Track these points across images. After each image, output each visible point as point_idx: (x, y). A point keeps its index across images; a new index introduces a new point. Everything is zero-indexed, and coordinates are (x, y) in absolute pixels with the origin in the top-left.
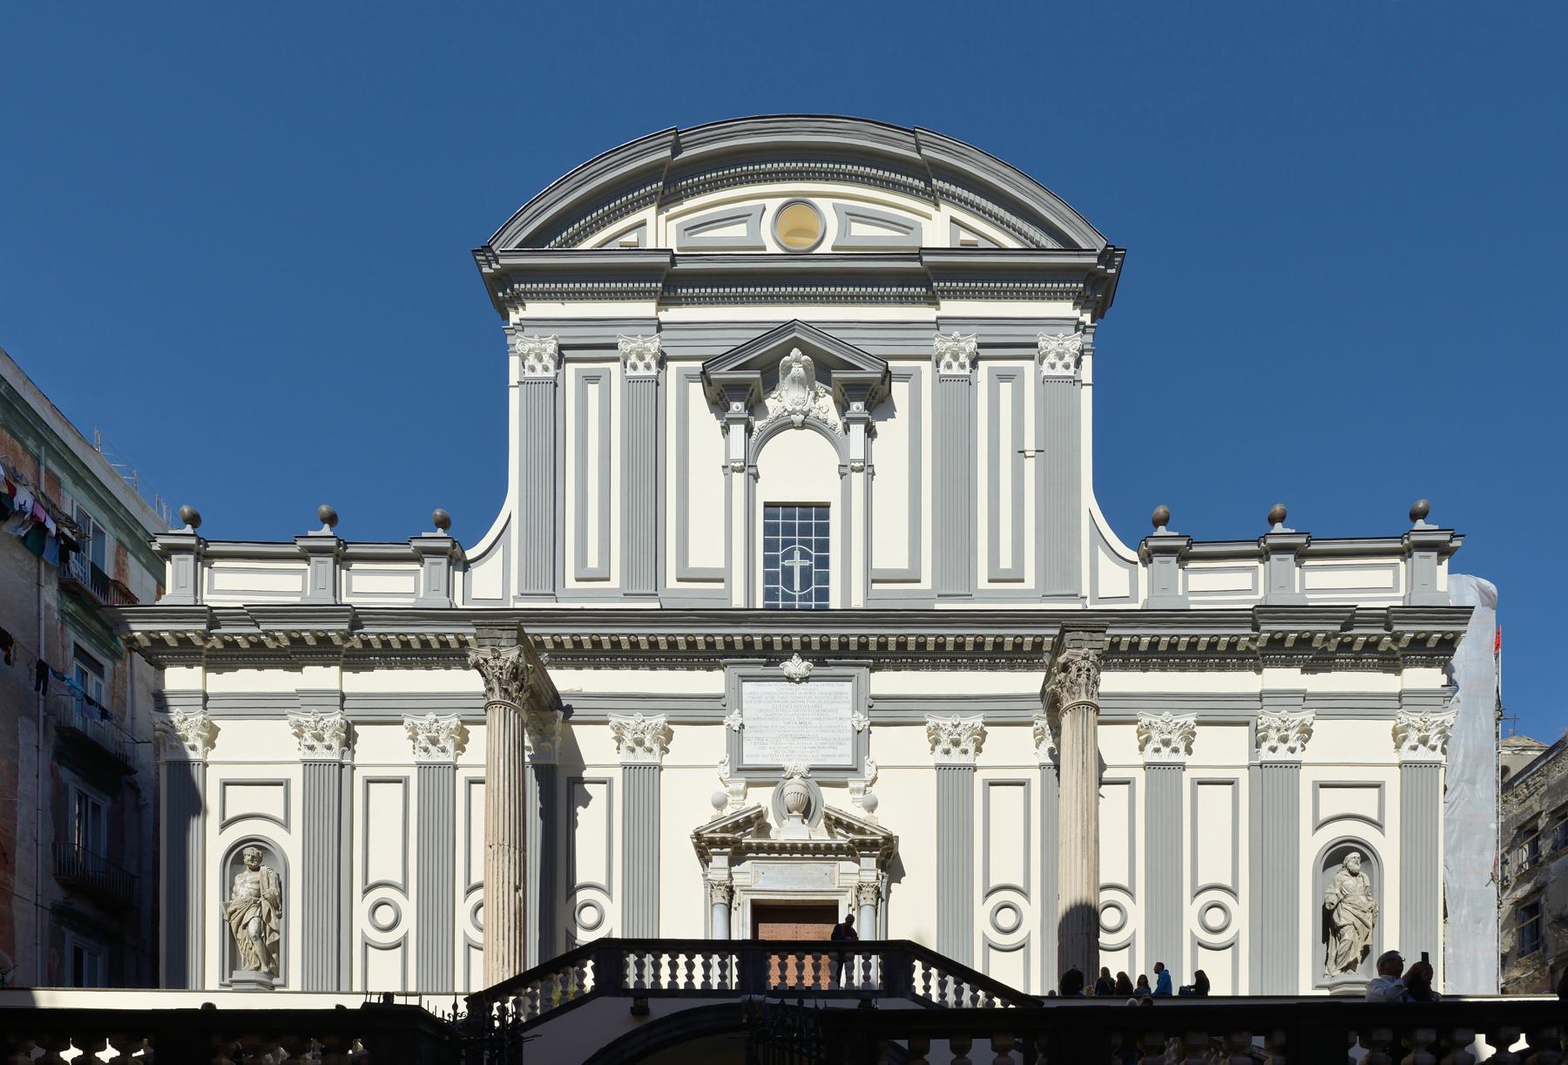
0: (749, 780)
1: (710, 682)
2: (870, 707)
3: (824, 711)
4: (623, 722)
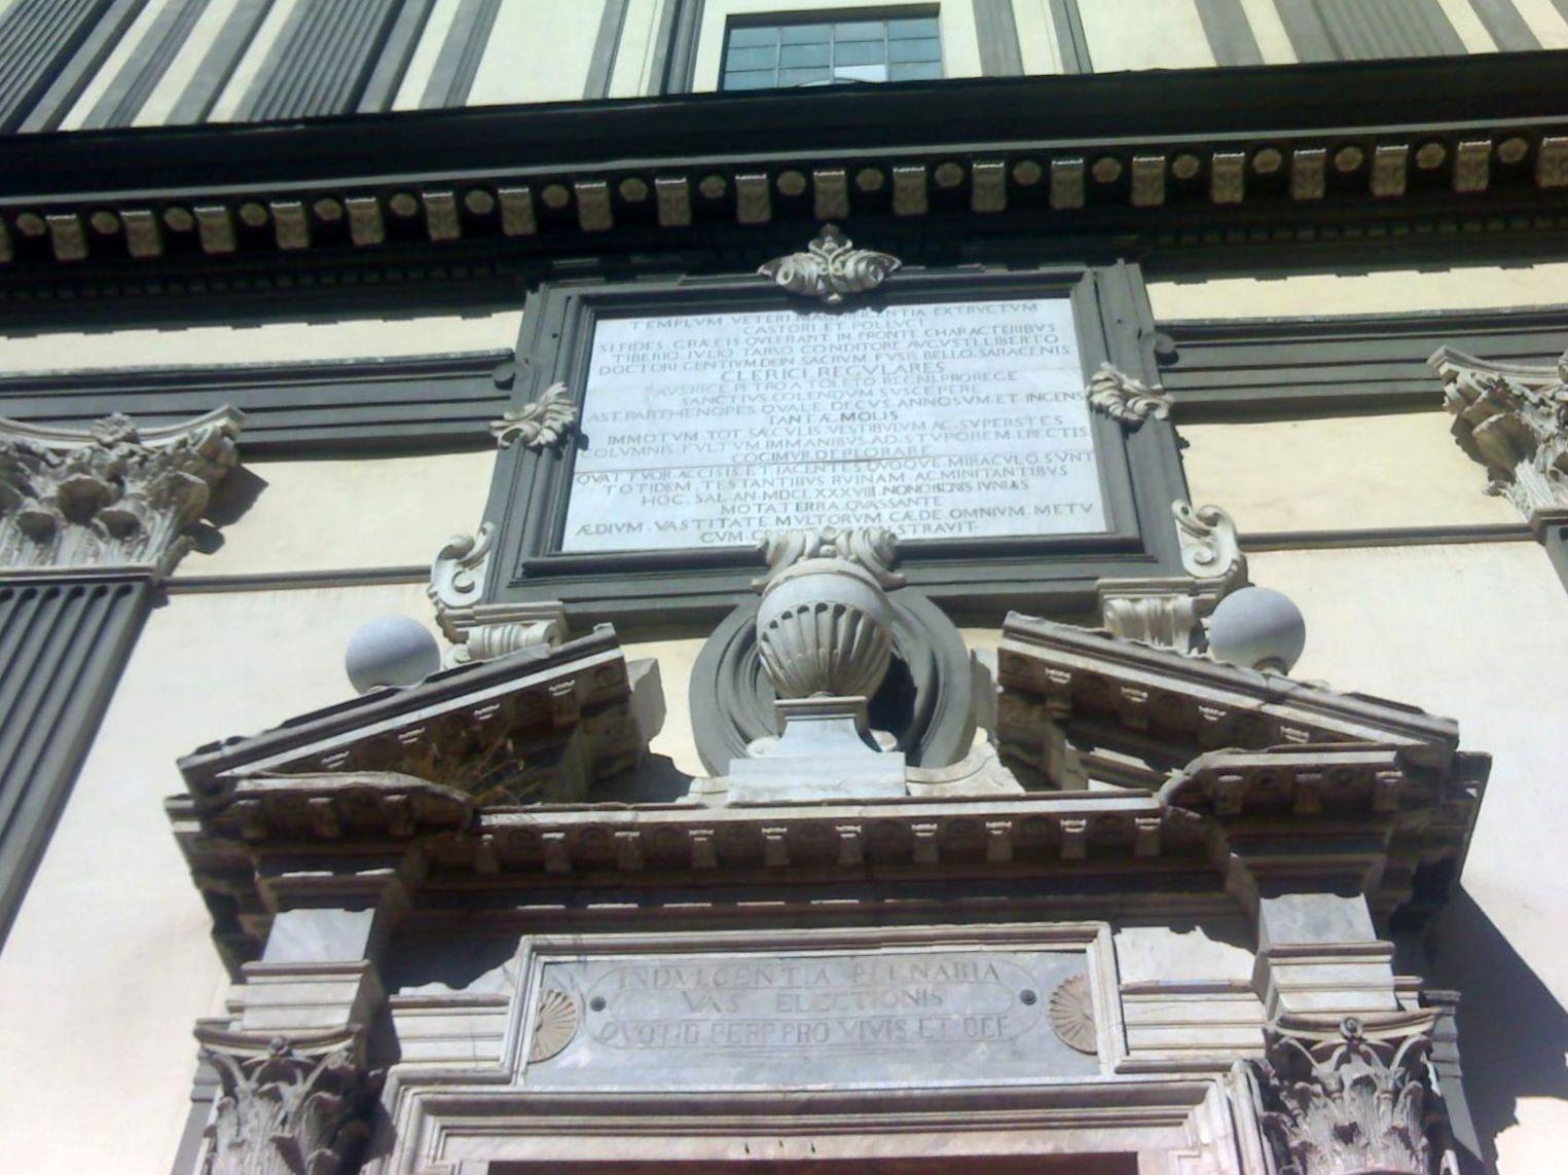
0: (573, 609)
3: (956, 377)
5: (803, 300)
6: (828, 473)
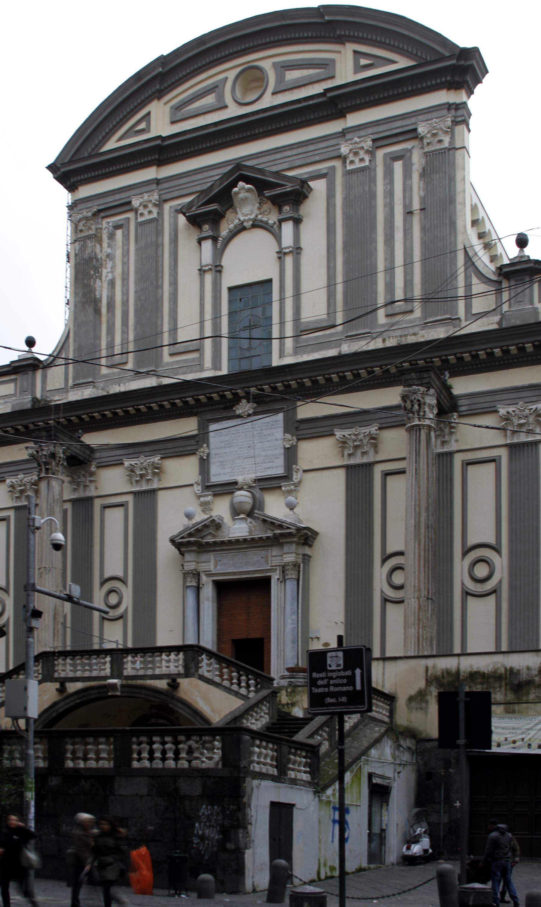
2: (296, 428)
3: (265, 436)
4: (133, 463)
5: (239, 416)
6: (246, 461)
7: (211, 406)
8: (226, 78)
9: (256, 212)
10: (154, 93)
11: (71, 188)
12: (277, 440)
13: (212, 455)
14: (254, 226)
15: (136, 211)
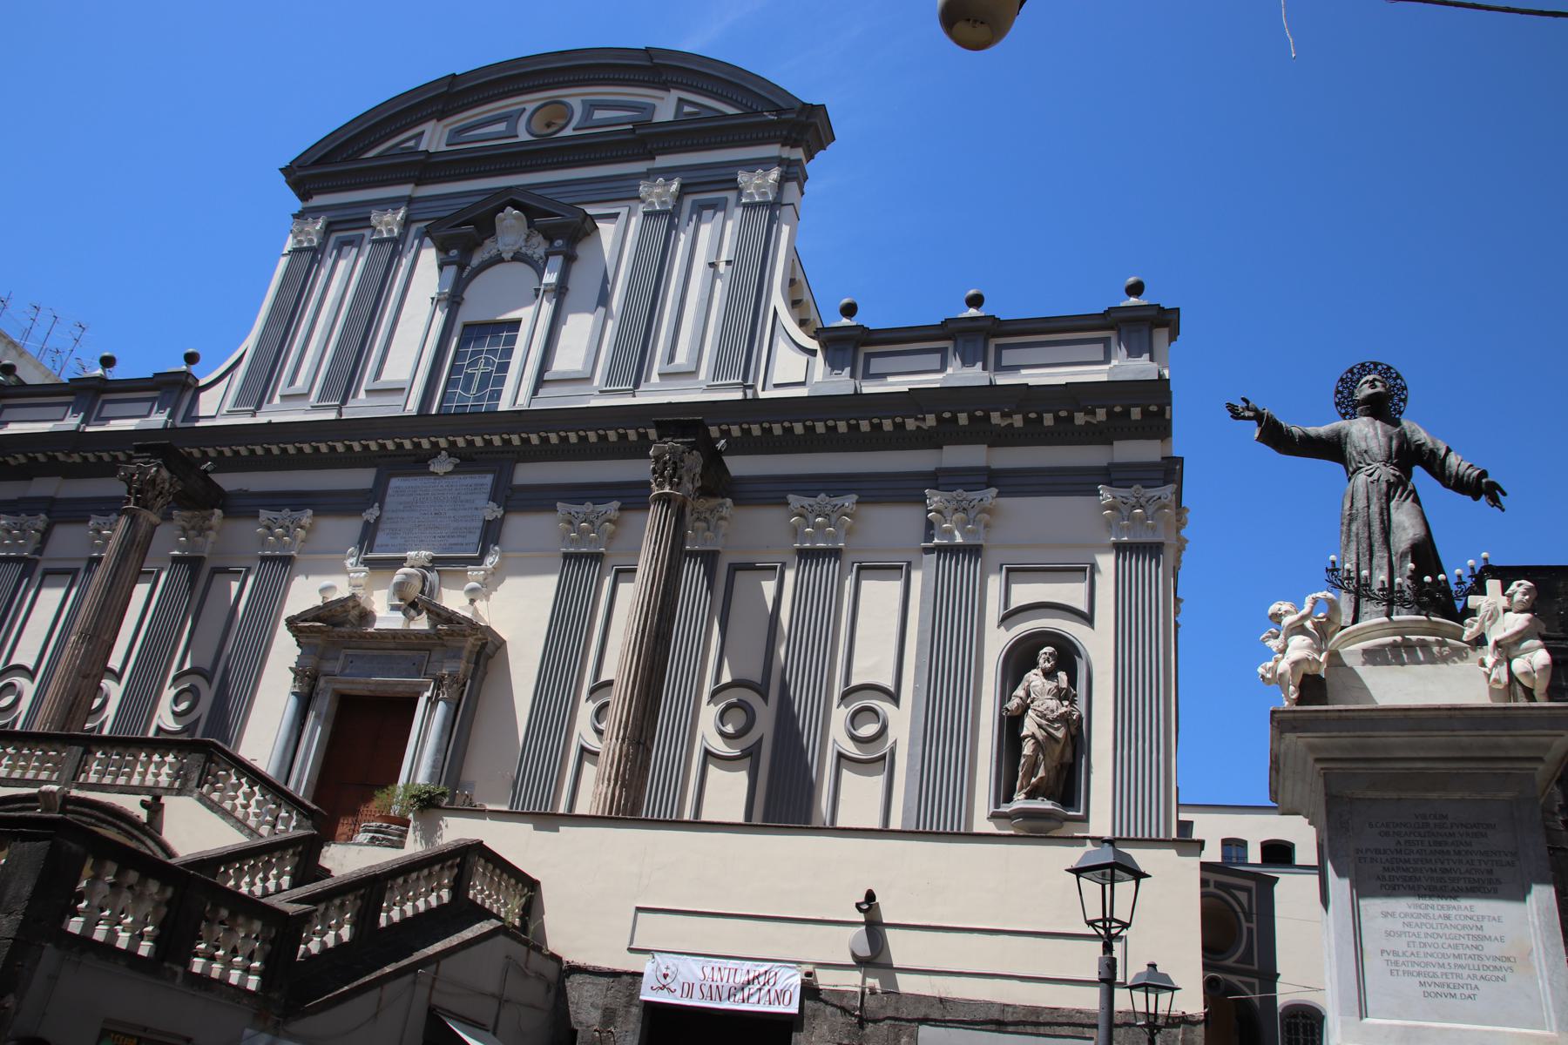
1: (362, 478)
3: (462, 502)
7: (399, 456)
8: (524, 109)
9: (521, 243)
10: (433, 113)
11: (304, 197)
12: (477, 509)
13: (384, 518)
14: (514, 259)
15: (374, 228)
